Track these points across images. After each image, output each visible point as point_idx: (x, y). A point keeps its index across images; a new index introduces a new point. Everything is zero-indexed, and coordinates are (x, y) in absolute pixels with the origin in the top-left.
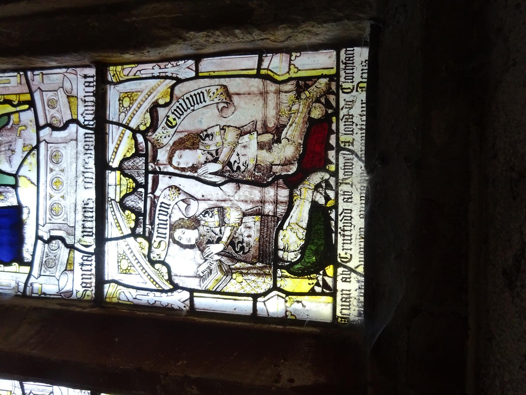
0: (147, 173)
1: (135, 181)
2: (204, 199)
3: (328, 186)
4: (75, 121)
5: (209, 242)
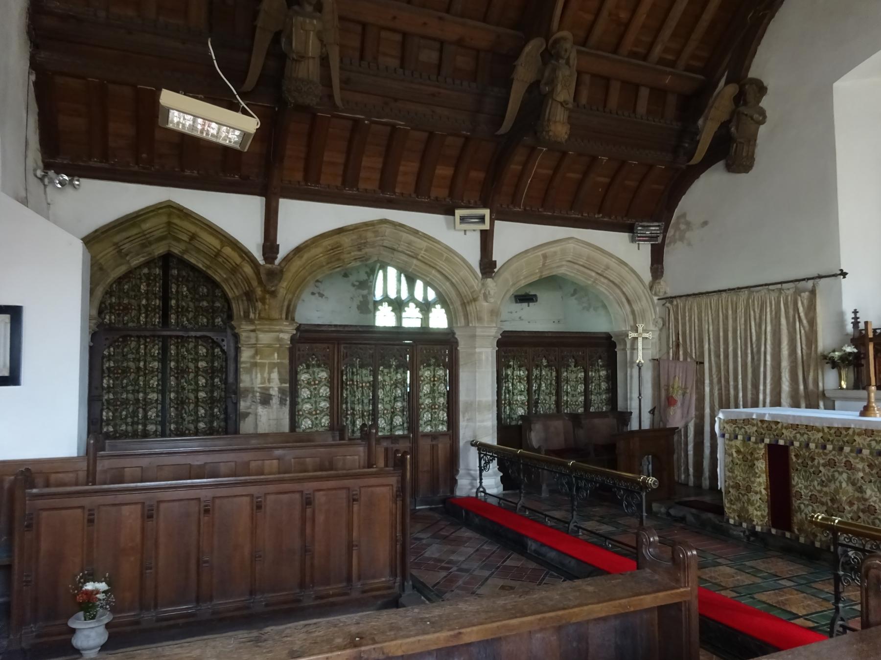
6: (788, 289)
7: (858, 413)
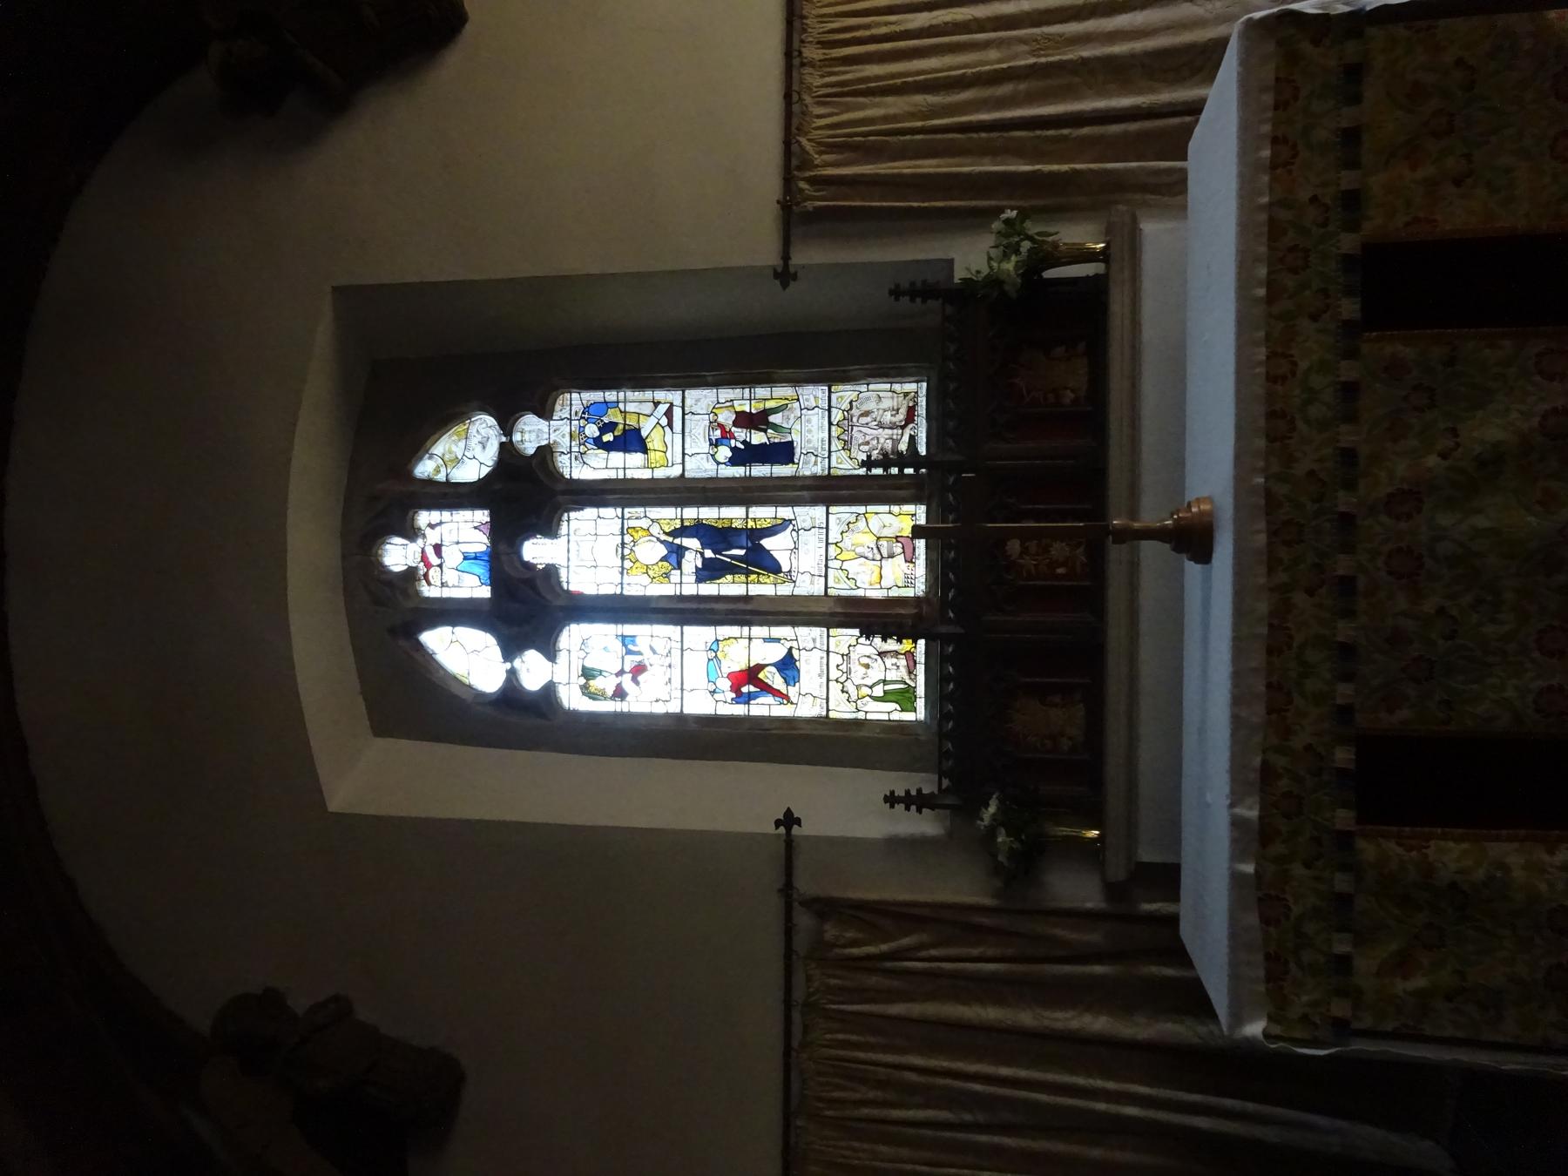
2: (871, 435)
6: (809, 979)
7: (1192, 569)
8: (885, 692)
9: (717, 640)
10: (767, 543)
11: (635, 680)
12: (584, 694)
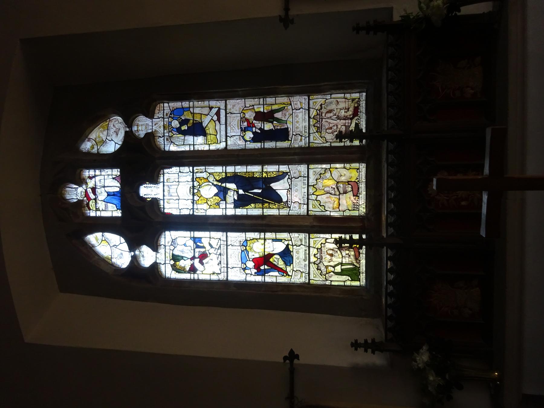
0: (320, 118)
1: (317, 120)
3: (358, 119)
4: (302, 108)
5: (334, 132)
8: (341, 269)
9: (246, 240)
10: (274, 186)
11: (201, 262)
12: (173, 269)
